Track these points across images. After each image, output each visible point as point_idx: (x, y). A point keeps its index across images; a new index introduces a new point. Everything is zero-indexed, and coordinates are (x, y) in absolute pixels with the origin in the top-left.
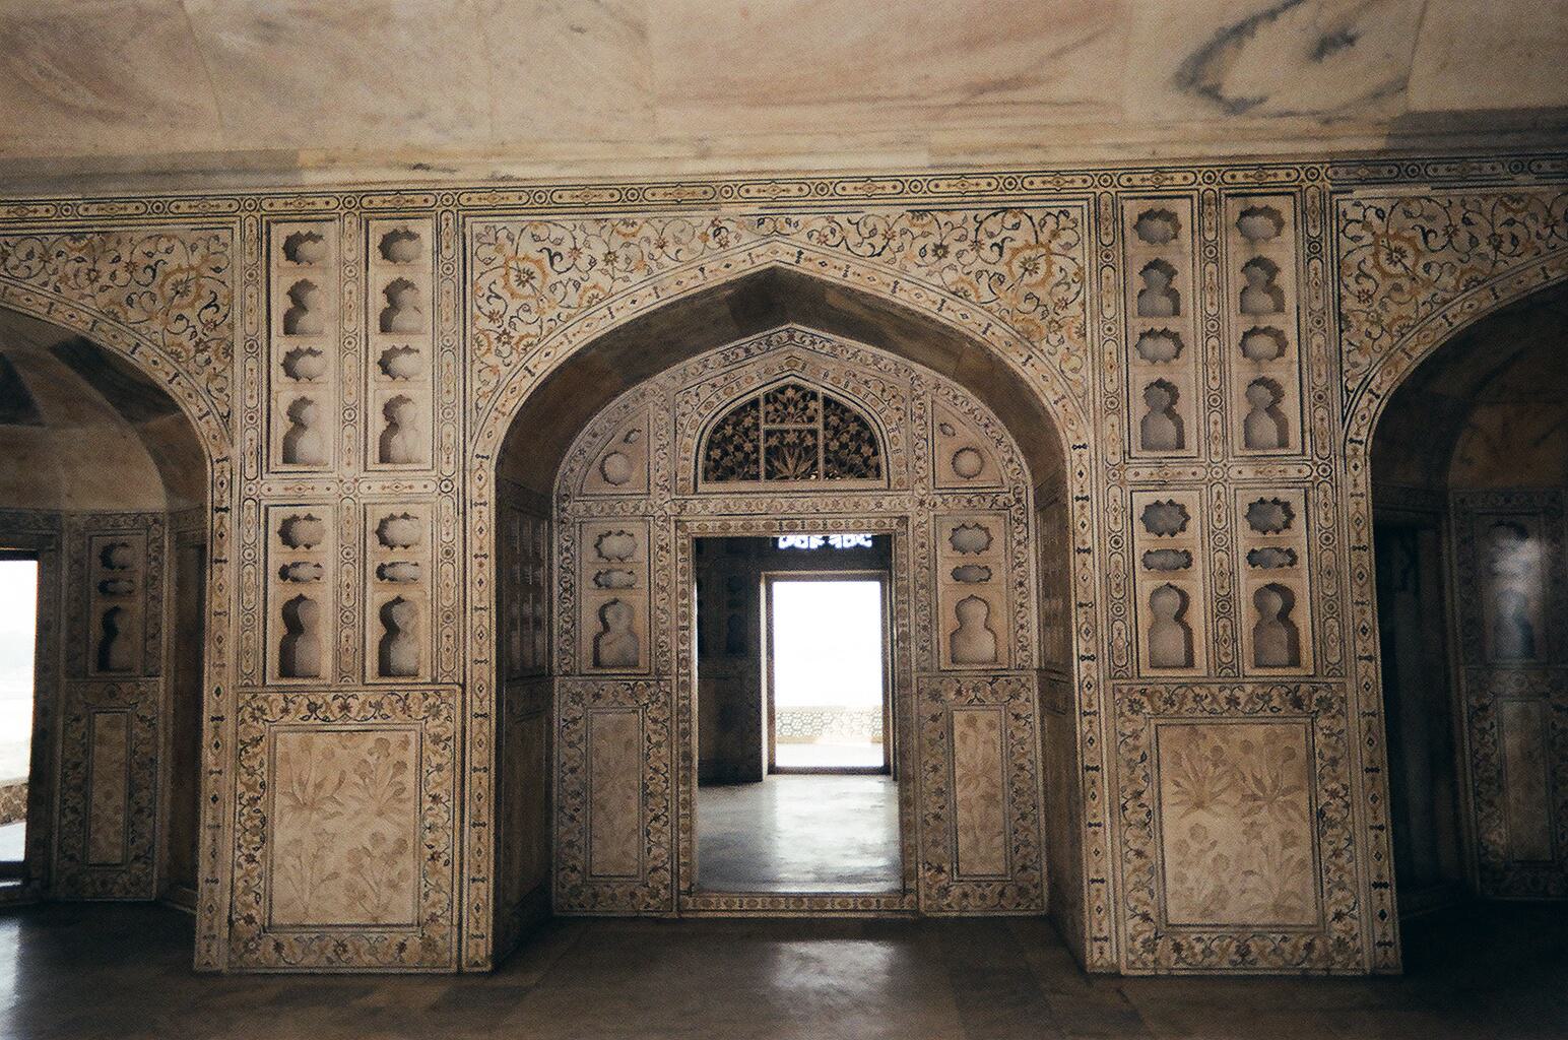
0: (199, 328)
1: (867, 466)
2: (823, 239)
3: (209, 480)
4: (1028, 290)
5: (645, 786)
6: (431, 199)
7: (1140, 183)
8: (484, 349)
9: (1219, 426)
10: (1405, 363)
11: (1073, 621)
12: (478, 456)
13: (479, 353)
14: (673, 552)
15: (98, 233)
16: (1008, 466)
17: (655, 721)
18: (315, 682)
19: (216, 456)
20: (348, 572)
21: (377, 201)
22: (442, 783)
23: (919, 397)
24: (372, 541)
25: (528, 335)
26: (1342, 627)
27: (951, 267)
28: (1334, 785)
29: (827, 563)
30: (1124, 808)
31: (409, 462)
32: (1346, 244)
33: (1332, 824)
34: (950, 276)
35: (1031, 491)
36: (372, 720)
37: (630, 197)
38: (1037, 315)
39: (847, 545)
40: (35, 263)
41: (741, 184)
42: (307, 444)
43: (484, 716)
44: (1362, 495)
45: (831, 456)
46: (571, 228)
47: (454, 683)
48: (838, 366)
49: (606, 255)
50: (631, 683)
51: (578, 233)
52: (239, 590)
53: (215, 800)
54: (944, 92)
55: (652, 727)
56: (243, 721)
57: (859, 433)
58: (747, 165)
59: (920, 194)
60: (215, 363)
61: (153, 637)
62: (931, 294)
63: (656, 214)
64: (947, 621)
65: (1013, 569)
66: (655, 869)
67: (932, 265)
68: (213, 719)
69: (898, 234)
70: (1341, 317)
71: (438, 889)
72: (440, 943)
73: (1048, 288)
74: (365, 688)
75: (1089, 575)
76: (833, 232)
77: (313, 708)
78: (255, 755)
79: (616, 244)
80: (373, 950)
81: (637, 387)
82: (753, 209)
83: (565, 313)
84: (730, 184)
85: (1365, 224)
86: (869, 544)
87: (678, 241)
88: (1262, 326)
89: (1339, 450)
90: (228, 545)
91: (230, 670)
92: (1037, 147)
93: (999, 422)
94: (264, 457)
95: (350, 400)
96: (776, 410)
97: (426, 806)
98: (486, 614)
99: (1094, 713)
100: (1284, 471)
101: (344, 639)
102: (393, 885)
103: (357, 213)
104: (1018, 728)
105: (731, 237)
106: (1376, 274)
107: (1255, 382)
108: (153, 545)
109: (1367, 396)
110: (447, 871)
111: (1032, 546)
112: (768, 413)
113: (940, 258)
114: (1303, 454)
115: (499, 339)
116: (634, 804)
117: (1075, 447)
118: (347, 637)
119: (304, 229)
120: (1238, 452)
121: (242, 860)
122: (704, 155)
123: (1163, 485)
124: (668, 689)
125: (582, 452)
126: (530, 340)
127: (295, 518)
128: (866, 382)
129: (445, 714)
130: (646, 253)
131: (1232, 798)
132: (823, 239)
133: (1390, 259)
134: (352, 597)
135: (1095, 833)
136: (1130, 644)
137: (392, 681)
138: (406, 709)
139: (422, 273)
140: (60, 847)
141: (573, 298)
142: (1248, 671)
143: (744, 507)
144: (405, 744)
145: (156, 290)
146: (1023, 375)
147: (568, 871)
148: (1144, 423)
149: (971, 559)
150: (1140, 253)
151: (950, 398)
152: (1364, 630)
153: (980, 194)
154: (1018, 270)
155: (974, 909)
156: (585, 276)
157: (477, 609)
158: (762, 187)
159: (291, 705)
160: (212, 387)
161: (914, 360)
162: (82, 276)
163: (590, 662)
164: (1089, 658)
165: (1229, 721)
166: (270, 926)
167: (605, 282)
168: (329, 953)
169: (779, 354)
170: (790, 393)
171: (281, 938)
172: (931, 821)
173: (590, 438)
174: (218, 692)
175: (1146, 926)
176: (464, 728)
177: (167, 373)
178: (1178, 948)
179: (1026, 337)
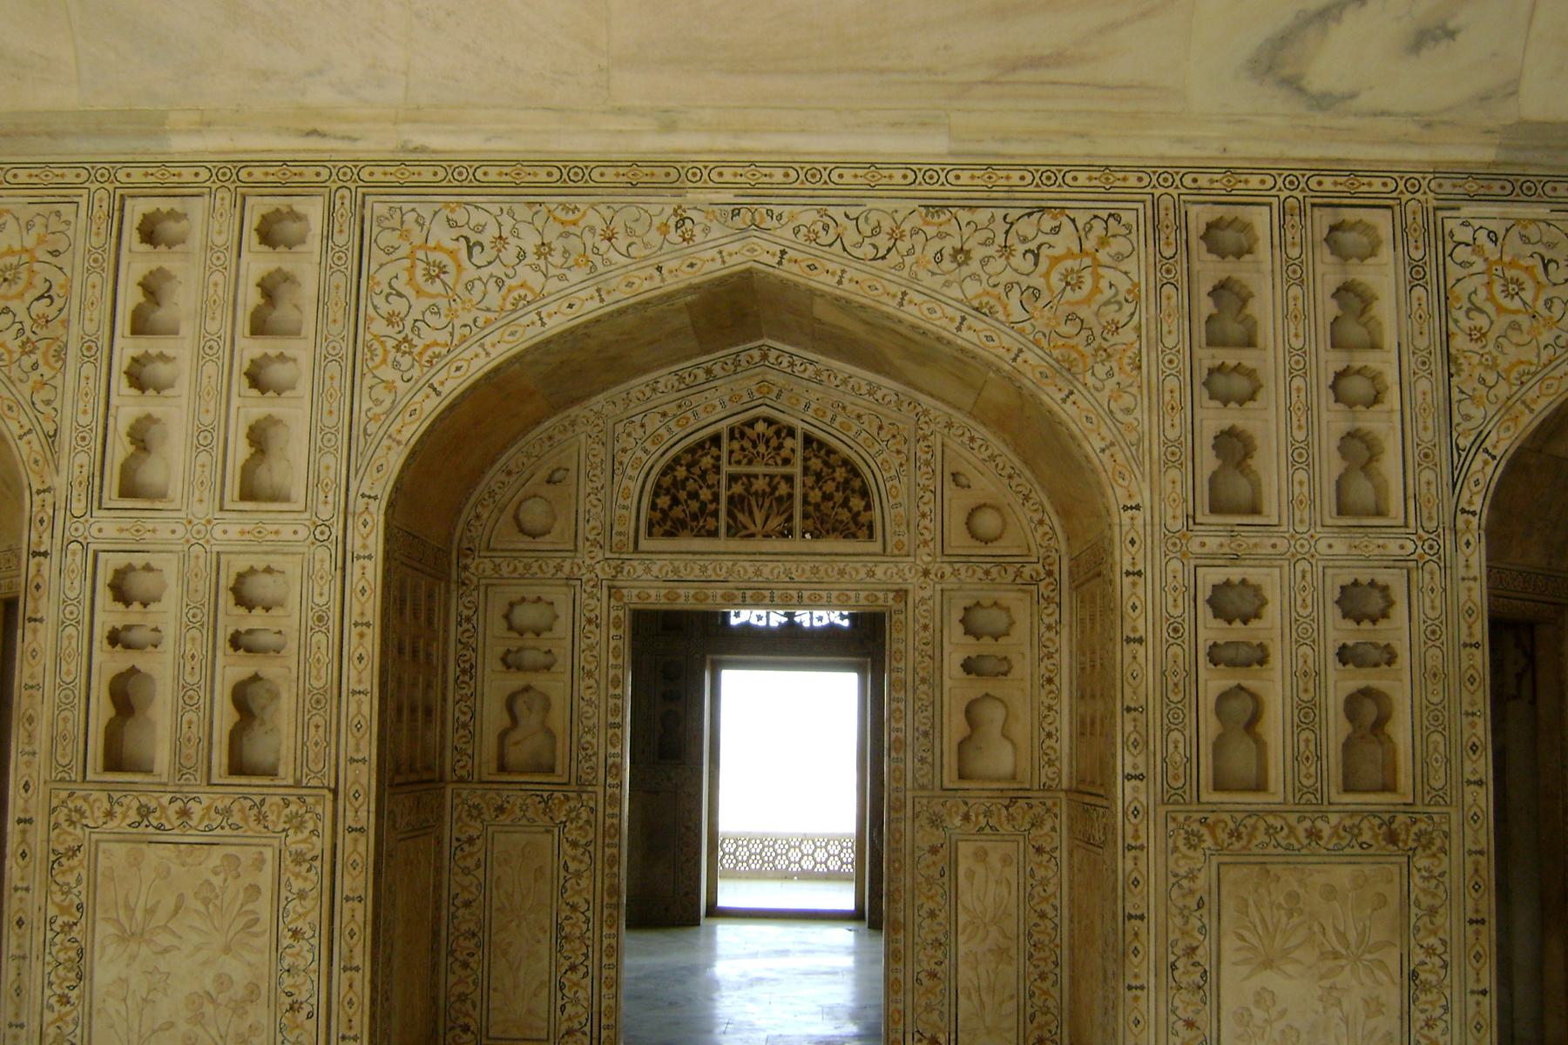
0: (28, 324)
1: (856, 523)
2: (812, 236)
3: (27, 515)
4: (1069, 309)
5: (560, 927)
6: (325, 173)
7: (1207, 185)
8: (378, 360)
9: (1305, 489)
10: (1526, 418)
11: (1119, 729)
12: (363, 496)
13: (371, 364)
14: (604, 628)
16: (1031, 527)
17: (575, 844)
18: (148, 779)
20: (194, 639)
21: (258, 174)
22: (306, 914)
23: (925, 438)
24: (226, 599)
25: (436, 344)
26: (1448, 742)
27: (972, 276)
28: (1432, 941)
29: (791, 647)
30: (1174, 967)
31: (274, 498)
32: (1454, 271)
33: (1426, 987)
34: (972, 288)
35: (1065, 561)
36: (218, 831)
37: (572, 177)
38: (1079, 341)
39: (817, 624)
41: (712, 165)
42: (151, 473)
43: (361, 830)
44: (1475, 579)
45: (811, 509)
46: (495, 209)
48: (823, 396)
49: (538, 248)
50: (545, 795)
52: (58, 660)
53: (20, 923)
55: (571, 852)
56: (57, 825)
57: (847, 481)
58: (722, 142)
59: (936, 187)
60: (43, 369)
62: (949, 311)
63: (606, 199)
64: (955, 727)
65: (1041, 660)
66: (570, 1032)
67: (949, 272)
68: (20, 821)
69: (907, 233)
70: (1450, 358)
73: (1095, 307)
74: (208, 789)
75: (1142, 669)
76: (826, 228)
77: (144, 812)
78: (71, 869)
81: (566, 413)
82: (727, 196)
84: (700, 165)
86: (846, 623)
87: (630, 232)
88: (1357, 365)
89: (1448, 519)
90: (45, 599)
91: (41, 758)
93: (1028, 474)
94: (96, 489)
95: (207, 419)
96: (743, 449)
97: (286, 942)
98: (365, 699)
99: (1141, 848)
100: (1384, 546)
101: (185, 726)
103: (232, 187)
104: (1040, 864)
105: (697, 230)
106: (1489, 308)
107: (1349, 434)
109: (1481, 456)
110: (310, 1025)
111: (1065, 632)
112: (731, 452)
113: (960, 265)
114: (1406, 526)
115: (398, 348)
116: (544, 949)
117: (1126, 508)
118: (190, 722)
119: (164, 205)
120: (1328, 521)
121: (53, 1001)
122: (670, 127)
123: (1235, 559)
124: (592, 804)
125: (492, 494)
126: (437, 350)
127: (130, 568)
128: (859, 417)
129: (310, 826)
130: (589, 245)
132: (812, 236)
133: (1506, 291)
134: (197, 670)
135: (1136, 998)
136: (1189, 760)
137: (243, 780)
139: (305, 266)
141: (494, 298)
142: (1335, 798)
143: (697, 571)
144: (263, 861)
146: (1063, 415)
147: (458, 1031)
148: (1213, 480)
149: (986, 646)
150: (1210, 269)
151: (965, 439)
152: (1474, 748)
153: (1011, 189)
154: (1056, 281)
156: (511, 272)
157: (354, 692)
158: (740, 171)
159: (116, 808)
161: (922, 391)
163: (493, 767)
164: (1136, 777)
165: (1310, 859)
167: (535, 280)
169: (749, 378)
170: (761, 427)
172: (926, 981)
173: (503, 477)
174: (26, 787)
176: (335, 846)
179: (1066, 368)
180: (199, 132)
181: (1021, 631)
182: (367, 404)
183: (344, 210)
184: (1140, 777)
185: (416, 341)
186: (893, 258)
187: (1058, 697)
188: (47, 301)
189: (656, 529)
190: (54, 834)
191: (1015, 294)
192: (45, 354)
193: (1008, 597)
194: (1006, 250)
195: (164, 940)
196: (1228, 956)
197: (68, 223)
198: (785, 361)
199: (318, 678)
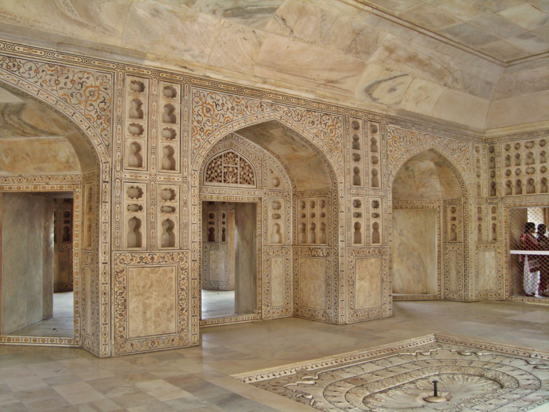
0: (98, 110)
6: (182, 78)
15: (60, 66)
19: (104, 161)
21: (165, 75)
25: (209, 130)
28: (385, 273)
34: (315, 131)
38: (332, 145)
40: (33, 73)
51: (224, 98)
53: (105, 294)
54: (321, 80)
56: (117, 264)
58: (273, 88)
60: (104, 125)
68: (103, 263)
70: (387, 156)
71: (184, 320)
72: (185, 337)
77: (141, 259)
78: (121, 277)
79: (234, 104)
80: (164, 343)
82: (270, 101)
83: (220, 124)
85: (391, 134)
87: (251, 107)
92: (337, 99)
93: (284, 171)
95: (154, 145)
97: (180, 292)
110: (186, 313)
111: (291, 208)
115: (200, 130)
118: (153, 232)
121: (118, 315)
122: (265, 83)
123: (358, 195)
127: (132, 187)
129: (185, 260)
131: (368, 277)
138: (173, 259)
141: (222, 120)
145: (82, 93)
155: (276, 316)
159: (134, 258)
160: (102, 134)
166: (129, 338)
167: (231, 116)
168: (149, 345)
170: (231, 154)
175: (352, 311)
177: (86, 126)
178: (357, 315)
180: (155, 61)
181: (283, 207)
182: (193, 145)
184: (343, 241)
186: (301, 121)
187: (290, 223)
188: (103, 104)
189: (208, 180)
190: (116, 267)
191: (322, 133)
192: (104, 120)
193: (281, 200)
194: (321, 123)
195: (147, 295)
196: (357, 278)
197: (109, 80)
198: (237, 138)
199: (185, 220)
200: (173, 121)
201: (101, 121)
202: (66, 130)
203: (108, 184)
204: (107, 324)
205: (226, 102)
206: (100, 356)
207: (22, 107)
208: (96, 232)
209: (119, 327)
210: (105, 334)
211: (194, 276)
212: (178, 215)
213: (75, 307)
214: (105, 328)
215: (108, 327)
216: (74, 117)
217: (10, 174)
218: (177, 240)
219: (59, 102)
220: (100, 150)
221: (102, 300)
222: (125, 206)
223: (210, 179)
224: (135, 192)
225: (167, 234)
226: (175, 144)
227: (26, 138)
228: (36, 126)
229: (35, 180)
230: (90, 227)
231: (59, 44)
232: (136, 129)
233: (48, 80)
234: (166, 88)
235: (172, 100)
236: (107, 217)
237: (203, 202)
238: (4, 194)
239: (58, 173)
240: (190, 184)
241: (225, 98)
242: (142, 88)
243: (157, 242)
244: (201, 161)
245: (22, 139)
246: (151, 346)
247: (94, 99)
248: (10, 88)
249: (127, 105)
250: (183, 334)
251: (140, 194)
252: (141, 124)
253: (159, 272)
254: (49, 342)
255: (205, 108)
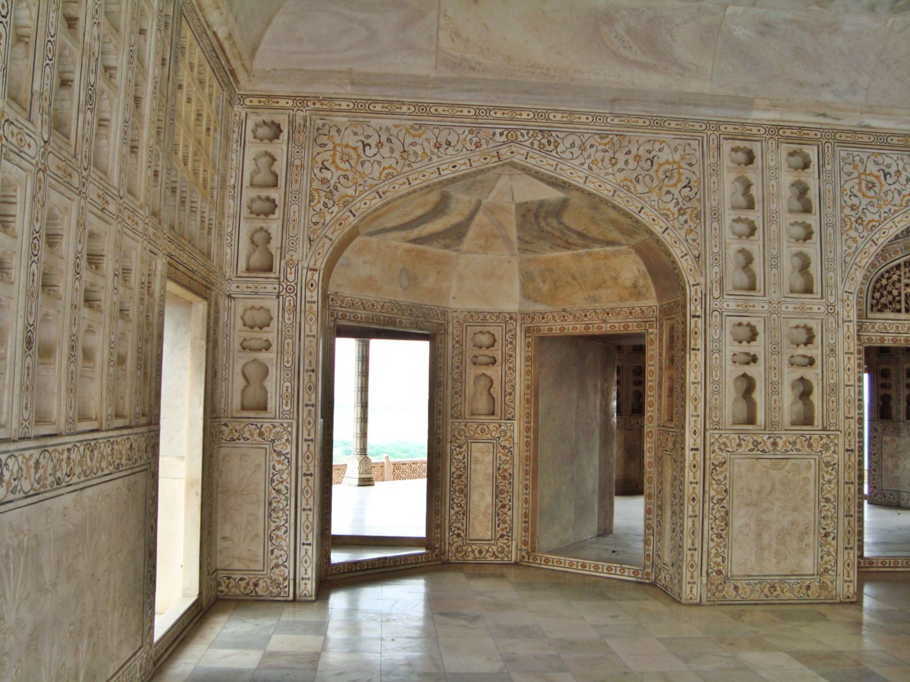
0: (680, 200)
8: (848, 227)
20: (775, 360)
21: (788, 132)
25: (873, 220)
36: (791, 452)
46: (895, 157)
47: (837, 430)
51: (900, 162)
53: (693, 499)
56: (714, 451)
60: (690, 223)
61: (510, 394)
68: (692, 450)
71: (829, 553)
72: (830, 585)
77: (756, 444)
78: (721, 472)
80: (791, 590)
95: (775, 252)
97: (822, 504)
98: (852, 389)
102: (804, 553)
108: (510, 334)
115: (856, 221)
118: (775, 400)
121: (714, 537)
126: (874, 223)
127: (740, 324)
129: (832, 449)
138: (810, 446)
140: (450, 528)
141: (897, 200)
144: (810, 466)
145: (654, 175)
159: (743, 442)
160: (689, 238)
162: (607, 162)
166: (732, 576)
168: (766, 591)
171: (738, 584)
174: (695, 433)
182: (845, 248)
183: (829, 153)
185: (864, 219)
188: (688, 189)
189: (874, 309)
190: (712, 456)
192: (691, 216)
195: (765, 505)
197: (695, 150)
199: (832, 379)
200: (807, 210)
201: (685, 217)
202: (631, 236)
203: (699, 320)
204: (695, 550)
205: (904, 168)
206: (683, 601)
207: (564, 205)
208: (680, 398)
209: (715, 556)
210: (692, 566)
211: (849, 478)
212: (819, 371)
213: (646, 519)
214: (692, 555)
215: (697, 554)
216: (642, 214)
217: (550, 309)
218: (817, 414)
219: (617, 193)
220: (685, 264)
221: (688, 509)
222: (729, 356)
223: (879, 307)
224: (745, 333)
225: (800, 402)
226: (812, 249)
227: (572, 252)
228: (584, 232)
229: (586, 316)
230: (671, 390)
231: (614, 101)
232: (742, 228)
233: (599, 160)
234: (791, 154)
235: (803, 174)
236: (699, 374)
237: (868, 351)
238: (542, 339)
239: (622, 305)
240: (841, 316)
241: (902, 160)
242: (750, 159)
243: (783, 417)
244: (859, 275)
245: (565, 254)
246: (769, 594)
247: (672, 182)
248: (545, 177)
249: (727, 188)
250: (827, 579)
251: (753, 337)
252: (751, 218)
253: (786, 468)
254: (605, 571)
255: (864, 183)
